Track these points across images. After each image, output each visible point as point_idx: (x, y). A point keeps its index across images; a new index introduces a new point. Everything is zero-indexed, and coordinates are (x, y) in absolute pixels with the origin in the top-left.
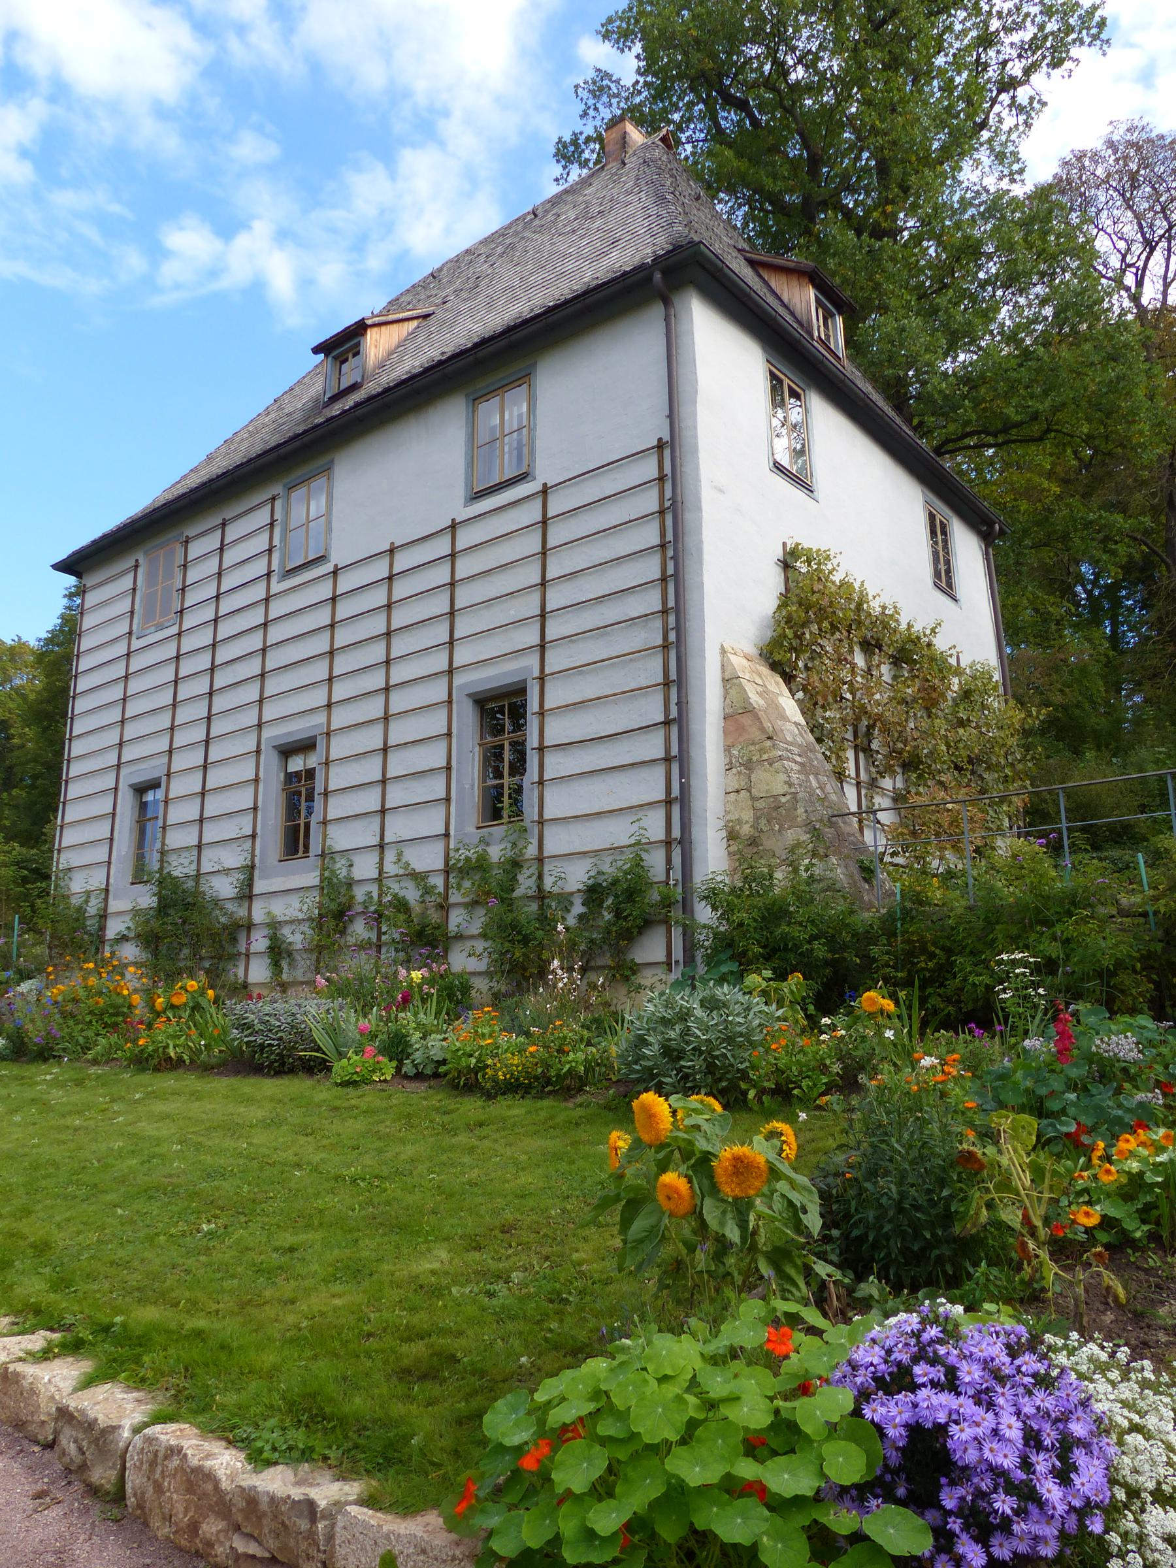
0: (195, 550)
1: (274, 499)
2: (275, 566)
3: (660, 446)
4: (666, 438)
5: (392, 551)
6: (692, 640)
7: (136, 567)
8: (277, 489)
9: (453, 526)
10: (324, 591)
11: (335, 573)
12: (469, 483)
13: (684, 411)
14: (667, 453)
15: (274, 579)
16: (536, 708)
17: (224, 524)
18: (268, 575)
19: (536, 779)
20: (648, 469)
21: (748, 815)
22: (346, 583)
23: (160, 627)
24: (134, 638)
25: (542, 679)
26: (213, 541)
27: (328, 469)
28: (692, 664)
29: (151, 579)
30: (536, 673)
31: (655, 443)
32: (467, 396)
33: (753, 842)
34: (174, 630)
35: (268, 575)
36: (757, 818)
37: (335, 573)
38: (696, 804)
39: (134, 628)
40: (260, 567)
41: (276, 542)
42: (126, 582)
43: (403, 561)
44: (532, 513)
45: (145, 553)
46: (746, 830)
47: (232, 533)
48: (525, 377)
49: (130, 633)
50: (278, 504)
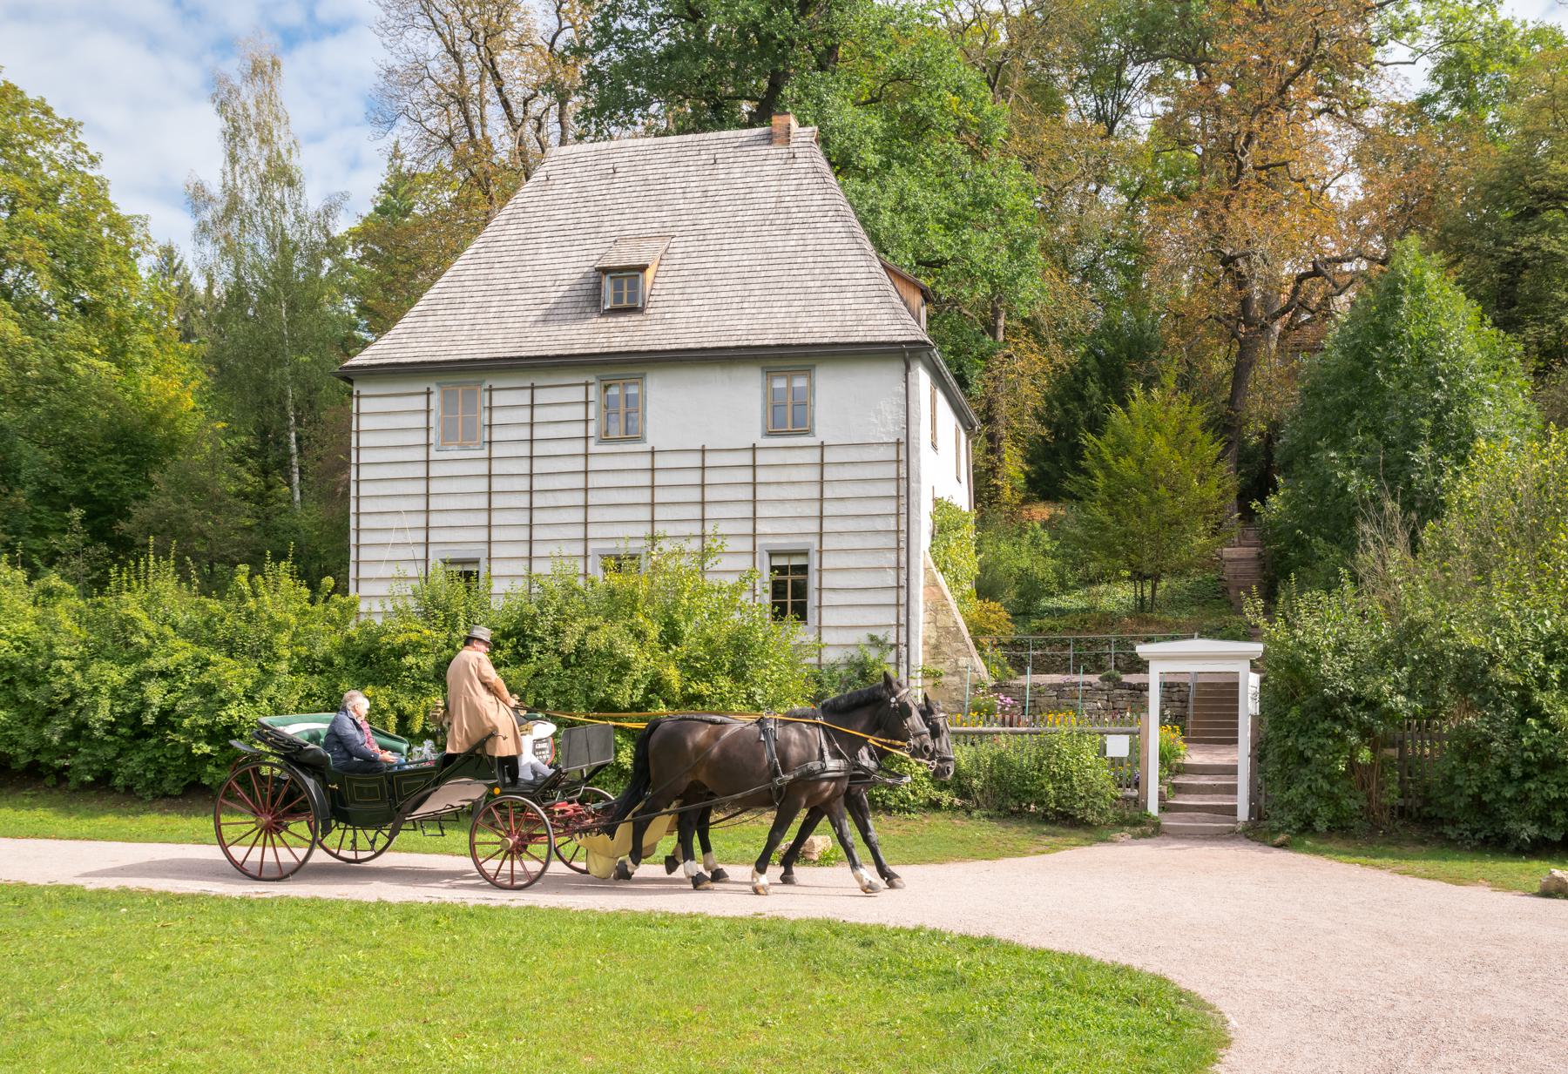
0: (499, 399)
1: (587, 385)
2: (592, 432)
3: (898, 443)
4: (903, 439)
5: (703, 451)
6: (913, 547)
7: (428, 393)
8: (592, 379)
9: (754, 448)
10: (645, 462)
11: (653, 452)
12: (765, 425)
13: (912, 428)
14: (903, 448)
15: (592, 442)
16: (816, 566)
17: (533, 388)
18: (586, 438)
19: (817, 604)
20: (890, 453)
21: (934, 634)
22: (660, 461)
23: (464, 448)
24: (432, 449)
25: (821, 552)
26: (523, 398)
27: (642, 377)
28: (912, 561)
29: (446, 407)
30: (817, 547)
31: (894, 440)
32: (763, 368)
33: (936, 647)
34: (485, 454)
35: (586, 438)
36: (939, 637)
37: (653, 452)
38: (912, 628)
39: (432, 440)
40: (578, 430)
41: (592, 415)
42: (420, 402)
43: (711, 460)
44: (814, 456)
45: (438, 384)
46: (933, 641)
47: (541, 396)
48: (808, 371)
49: (428, 445)
50: (592, 389)
